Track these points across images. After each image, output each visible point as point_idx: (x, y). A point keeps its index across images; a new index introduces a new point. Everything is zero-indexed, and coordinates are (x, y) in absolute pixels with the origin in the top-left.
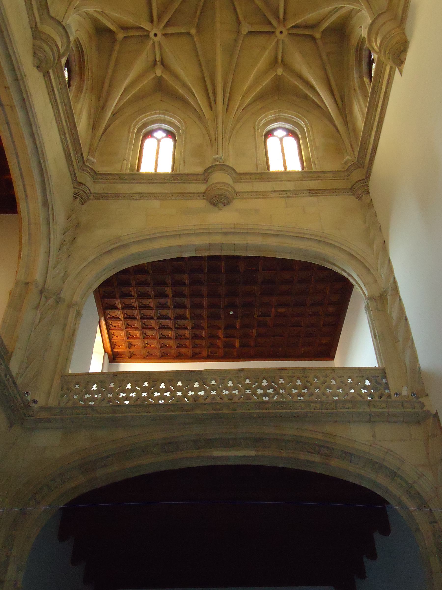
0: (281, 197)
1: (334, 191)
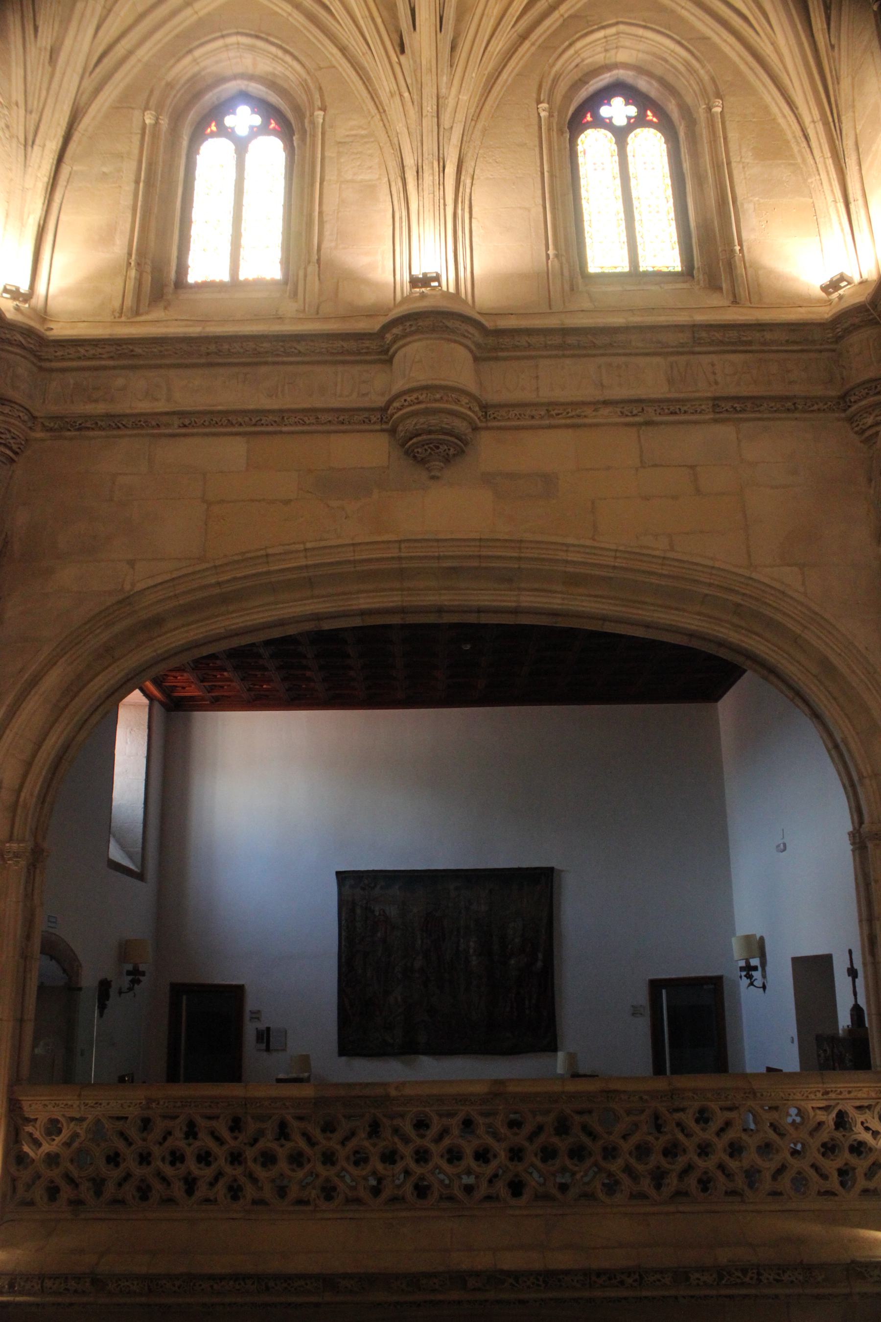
0: (627, 425)
1: (787, 405)
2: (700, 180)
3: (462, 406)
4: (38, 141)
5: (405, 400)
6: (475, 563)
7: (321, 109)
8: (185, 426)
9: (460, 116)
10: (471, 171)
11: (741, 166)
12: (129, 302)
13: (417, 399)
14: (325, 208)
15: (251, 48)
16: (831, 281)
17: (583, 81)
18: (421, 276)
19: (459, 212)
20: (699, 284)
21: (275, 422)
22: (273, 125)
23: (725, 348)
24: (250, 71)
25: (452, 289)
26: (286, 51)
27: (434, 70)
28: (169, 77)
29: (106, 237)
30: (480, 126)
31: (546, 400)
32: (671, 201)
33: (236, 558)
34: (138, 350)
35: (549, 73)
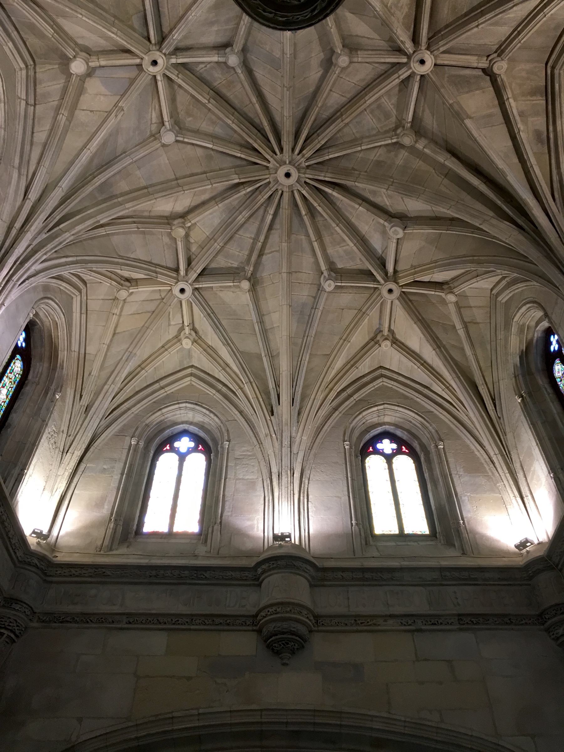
0: (406, 631)
1: (505, 620)
2: (435, 483)
3: (303, 616)
4: (70, 451)
5: (268, 611)
6: (310, 728)
7: (227, 441)
8: (130, 623)
9: (303, 447)
10: (308, 476)
11: (458, 476)
12: (106, 542)
13: (276, 611)
14: (226, 493)
15: (193, 409)
16: (521, 542)
17: (367, 430)
18: (280, 534)
19: (302, 498)
20: (440, 542)
21: (187, 622)
22: (200, 447)
23: (461, 582)
24: (191, 420)
25: (297, 543)
26: (211, 412)
27: (289, 424)
28: (147, 422)
29: (99, 504)
30: (313, 452)
31: (354, 613)
32: (420, 494)
33: (151, 719)
34: (108, 573)
35: (350, 426)
